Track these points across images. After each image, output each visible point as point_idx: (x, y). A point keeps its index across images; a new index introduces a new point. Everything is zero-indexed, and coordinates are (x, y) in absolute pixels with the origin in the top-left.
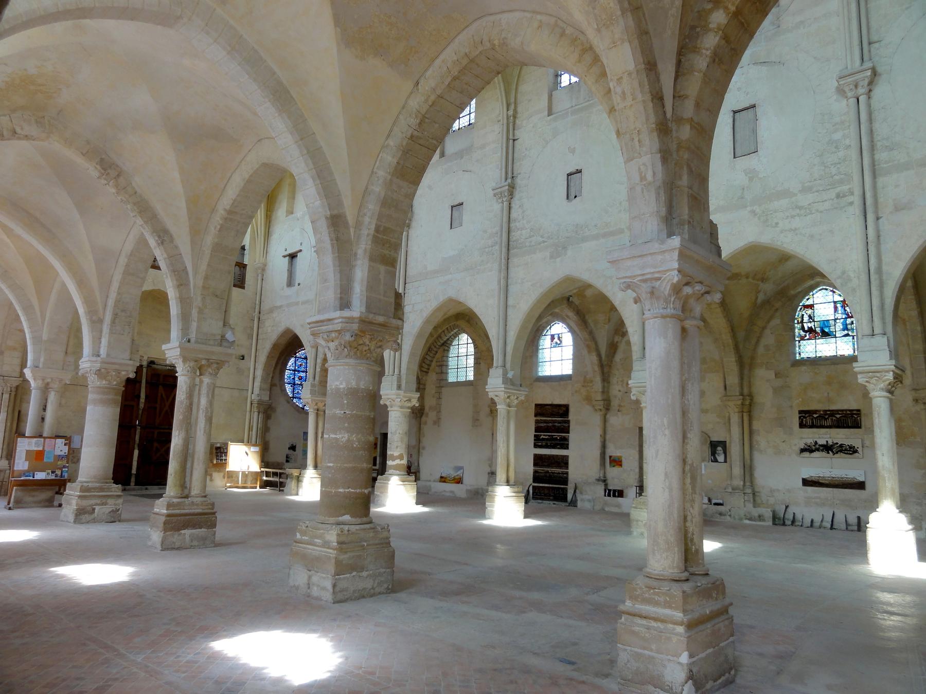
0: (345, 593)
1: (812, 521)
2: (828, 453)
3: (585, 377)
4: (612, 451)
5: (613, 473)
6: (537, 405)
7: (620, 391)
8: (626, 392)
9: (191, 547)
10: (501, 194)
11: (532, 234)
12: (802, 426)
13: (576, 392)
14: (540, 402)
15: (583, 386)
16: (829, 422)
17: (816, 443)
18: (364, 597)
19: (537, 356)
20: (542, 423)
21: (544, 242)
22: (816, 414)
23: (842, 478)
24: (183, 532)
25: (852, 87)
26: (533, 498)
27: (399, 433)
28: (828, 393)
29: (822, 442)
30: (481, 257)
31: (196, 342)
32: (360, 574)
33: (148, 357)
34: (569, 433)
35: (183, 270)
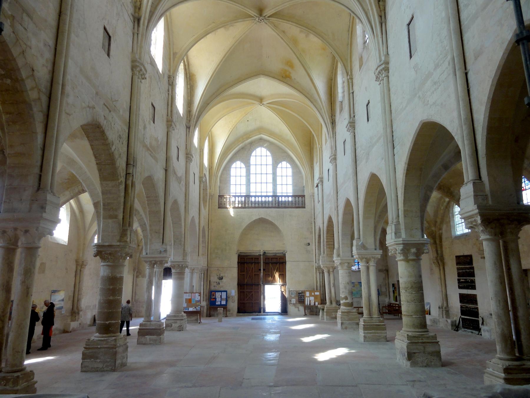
0: (87, 368)
6: (456, 257)
9: (150, 344)
14: (458, 254)
18: (97, 371)
19: (454, 220)
20: (460, 270)
21: (364, 153)
24: (146, 337)
26: (464, 327)
27: (343, 283)
31: (149, 254)
32: (96, 360)
33: (263, 250)
34: (474, 277)
35: (144, 224)
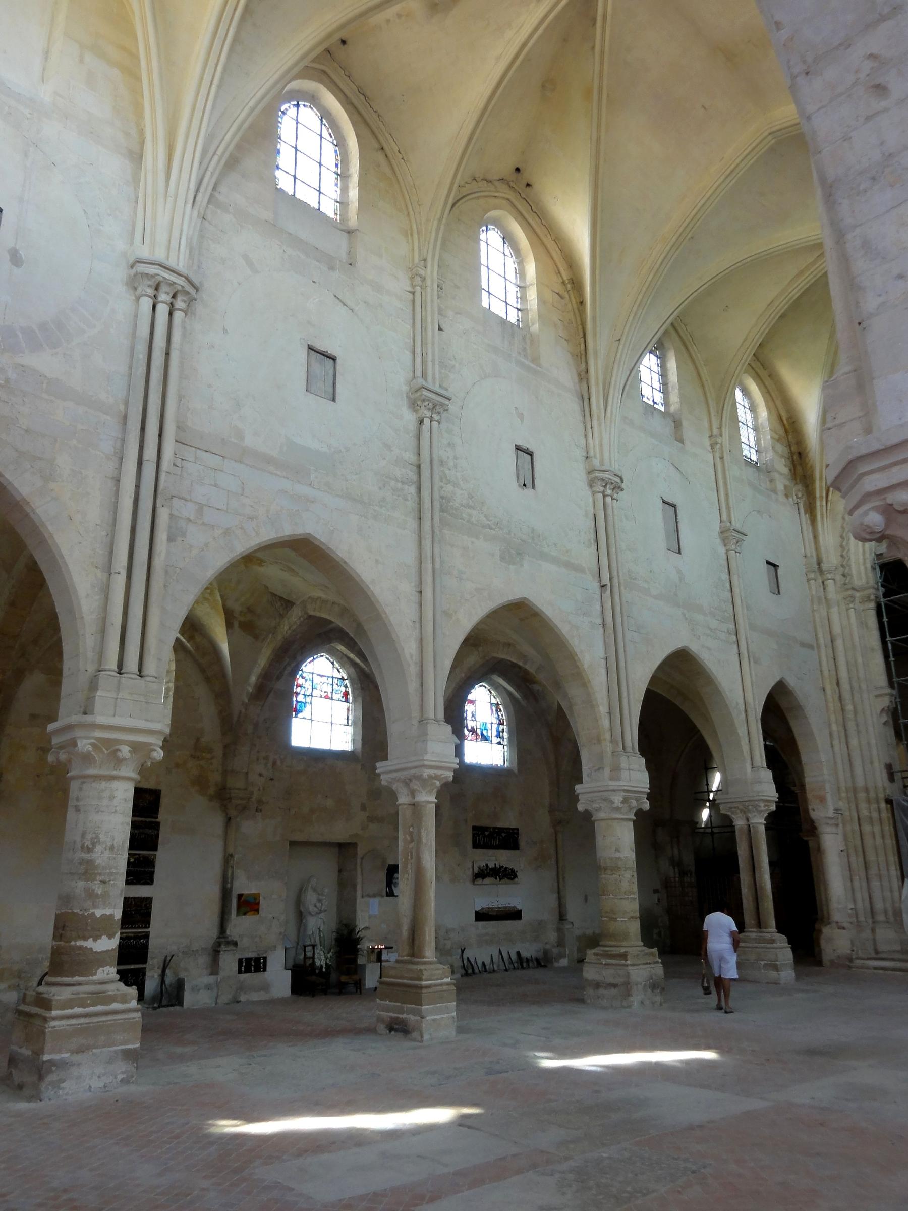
1: (483, 963)
2: (496, 879)
3: (198, 740)
4: (243, 885)
5: (239, 926)
7: (261, 775)
8: (272, 779)
10: (435, 406)
11: (471, 503)
12: (476, 845)
13: (177, 766)
15: (193, 757)
16: (496, 843)
17: (487, 865)
22: (487, 831)
23: (506, 907)
25: (735, 541)
28: (495, 808)
29: (491, 866)
30: (380, 489)
34: (156, 849)
